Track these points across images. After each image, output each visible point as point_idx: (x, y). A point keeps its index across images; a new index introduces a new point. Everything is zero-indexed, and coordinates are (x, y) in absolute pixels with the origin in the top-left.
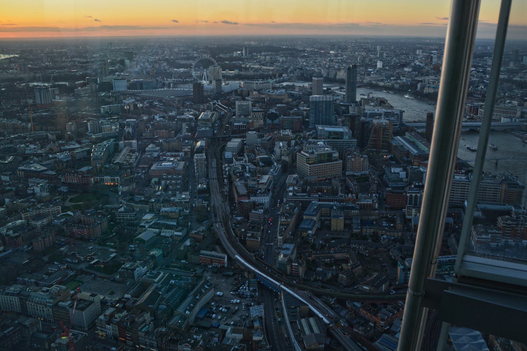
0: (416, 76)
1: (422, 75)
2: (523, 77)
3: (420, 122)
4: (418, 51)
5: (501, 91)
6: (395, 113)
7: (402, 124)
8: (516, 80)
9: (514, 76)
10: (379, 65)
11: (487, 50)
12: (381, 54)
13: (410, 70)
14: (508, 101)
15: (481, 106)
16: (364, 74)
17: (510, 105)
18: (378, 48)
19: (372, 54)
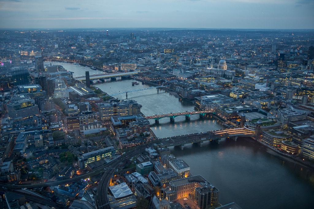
0: (79, 51)
1: (82, 50)
2: (136, 48)
3: (83, 77)
4: (79, 36)
5: (126, 56)
6: (68, 73)
7: (73, 79)
8: (133, 50)
9: (132, 48)
10: (56, 46)
11: (117, 34)
12: (57, 39)
13: (75, 48)
14: (130, 61)
15: (116, 65)
16: (47, 52)
17: (131, 63)
18: (55, 36)
19: (51, 40)
